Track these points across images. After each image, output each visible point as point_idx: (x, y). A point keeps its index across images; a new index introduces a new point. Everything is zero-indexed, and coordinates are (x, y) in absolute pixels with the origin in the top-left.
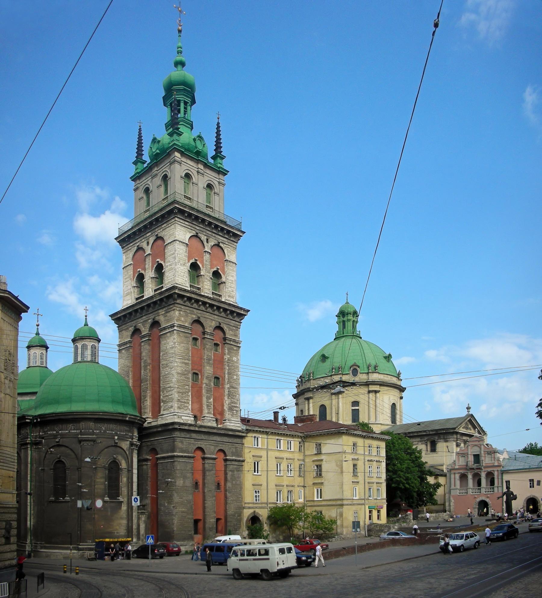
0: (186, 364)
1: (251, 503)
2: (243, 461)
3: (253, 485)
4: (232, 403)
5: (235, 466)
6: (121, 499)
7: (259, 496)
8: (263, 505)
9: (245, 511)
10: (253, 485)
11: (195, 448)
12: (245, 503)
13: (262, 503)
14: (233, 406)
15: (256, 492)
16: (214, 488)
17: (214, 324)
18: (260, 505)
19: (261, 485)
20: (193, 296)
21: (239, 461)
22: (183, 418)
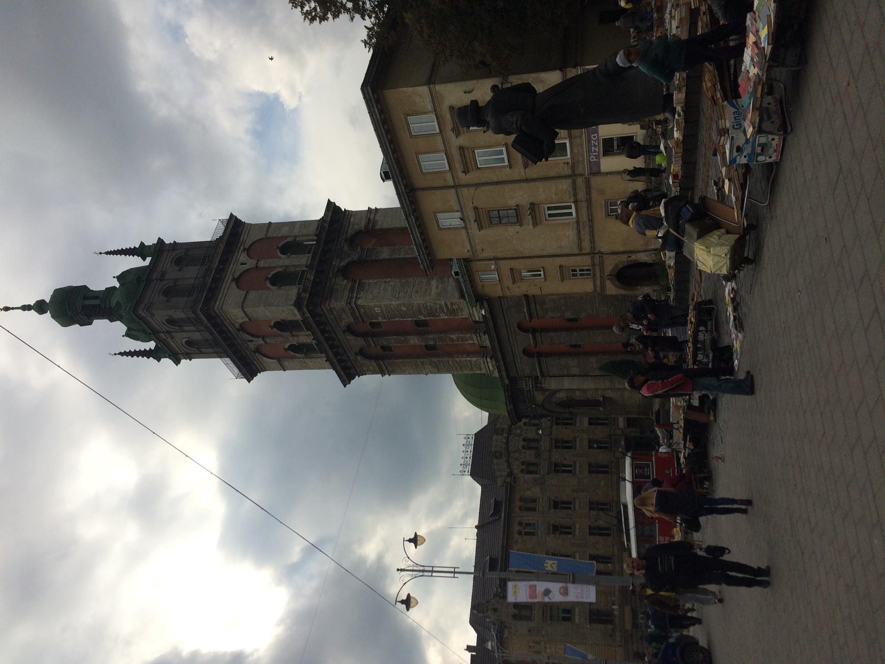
0: (423, 364)
1: (594, 282)
2: (526, 296)
3: (563, 280)
4: (443, 310)
5: (538, 307)
6: (601, 399)
7: (580, 270)
8: (597, 261)
9: (608, 292)
10: (563, 280)
11: (525, 357)
12: (595, 291)
13: (594, 265)
14: (448, 310)
15: (573, 275)
16: (575, 334)
17: (350, 337)
18: (597, 268)
19: (561, 266)
20: (339, 368)
21: (528, 305)
22: (491, 368)
